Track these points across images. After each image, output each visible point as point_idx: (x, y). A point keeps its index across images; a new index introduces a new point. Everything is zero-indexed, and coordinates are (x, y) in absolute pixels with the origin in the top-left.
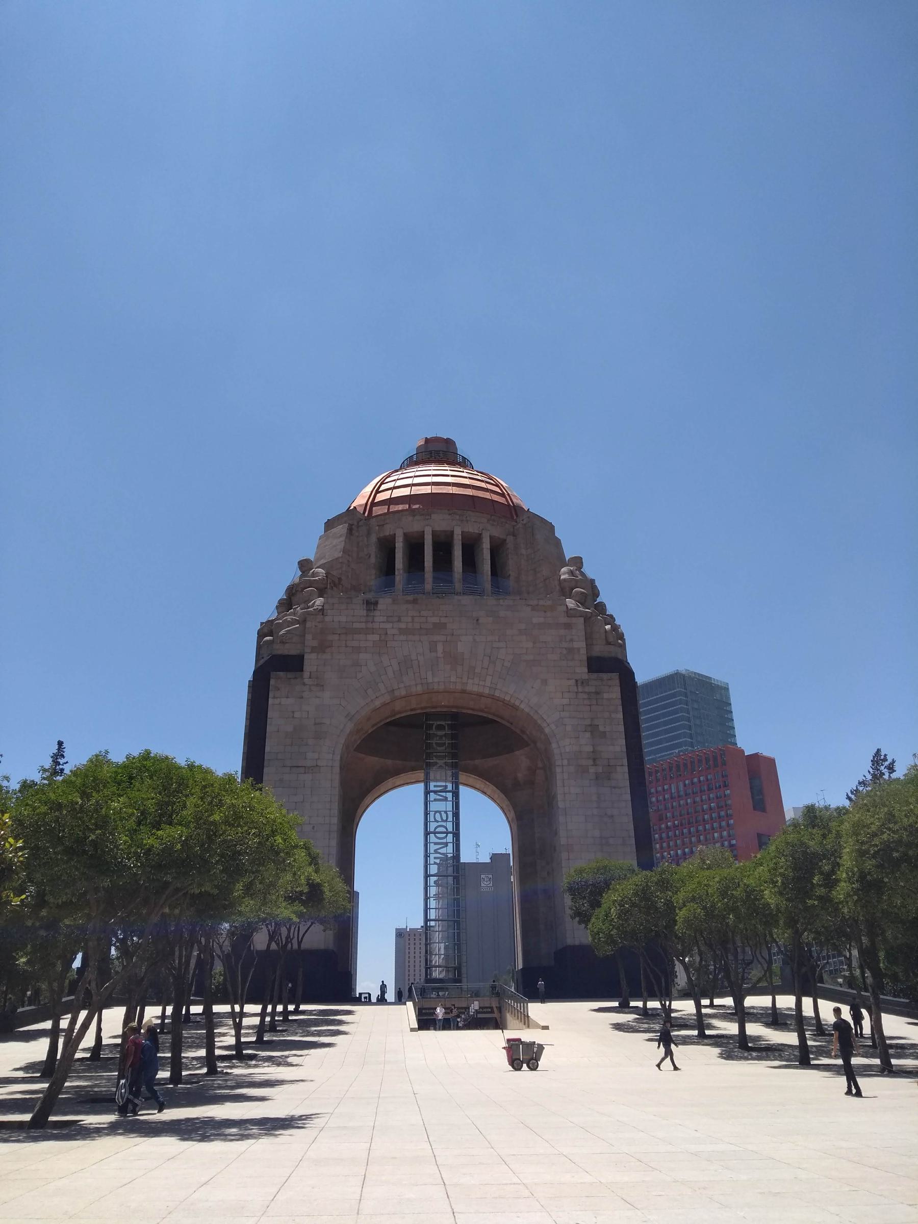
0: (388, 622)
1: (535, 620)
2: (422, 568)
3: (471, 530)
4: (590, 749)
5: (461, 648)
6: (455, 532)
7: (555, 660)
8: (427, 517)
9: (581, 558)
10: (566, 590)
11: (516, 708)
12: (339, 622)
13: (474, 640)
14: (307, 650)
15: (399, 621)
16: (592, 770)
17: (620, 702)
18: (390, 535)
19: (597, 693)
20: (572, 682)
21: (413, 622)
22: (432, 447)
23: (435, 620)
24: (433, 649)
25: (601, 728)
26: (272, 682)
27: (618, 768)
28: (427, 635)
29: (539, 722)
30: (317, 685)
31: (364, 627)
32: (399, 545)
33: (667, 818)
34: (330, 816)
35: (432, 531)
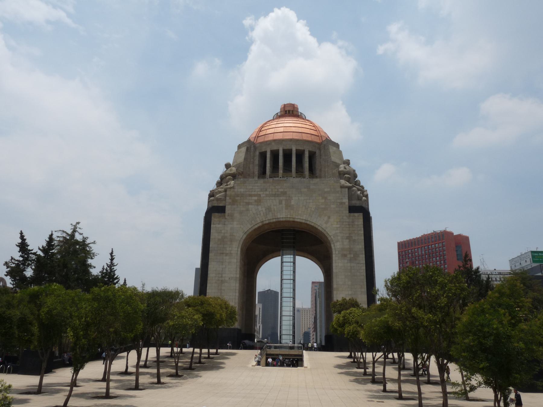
0: (261, 191)
1: (326, 190)
3: (300, 148)
4: (348, 247)
5: (293, 202)
6: (293, 150)
9: (349, 160)
10: (342, 175)
11: (316, 229)
12: (241, 192)
14: (227, 204)
15: (266, 190)
17: (362, 226)
18: (265, 151)
22: (287, 109)
25: (354, 238)
26: (212, 218)
28: (278, 197)
29: (326, 235)
32: (268, 155)
33: (416, 264)
34: (236, 274)
35: (283, 149)
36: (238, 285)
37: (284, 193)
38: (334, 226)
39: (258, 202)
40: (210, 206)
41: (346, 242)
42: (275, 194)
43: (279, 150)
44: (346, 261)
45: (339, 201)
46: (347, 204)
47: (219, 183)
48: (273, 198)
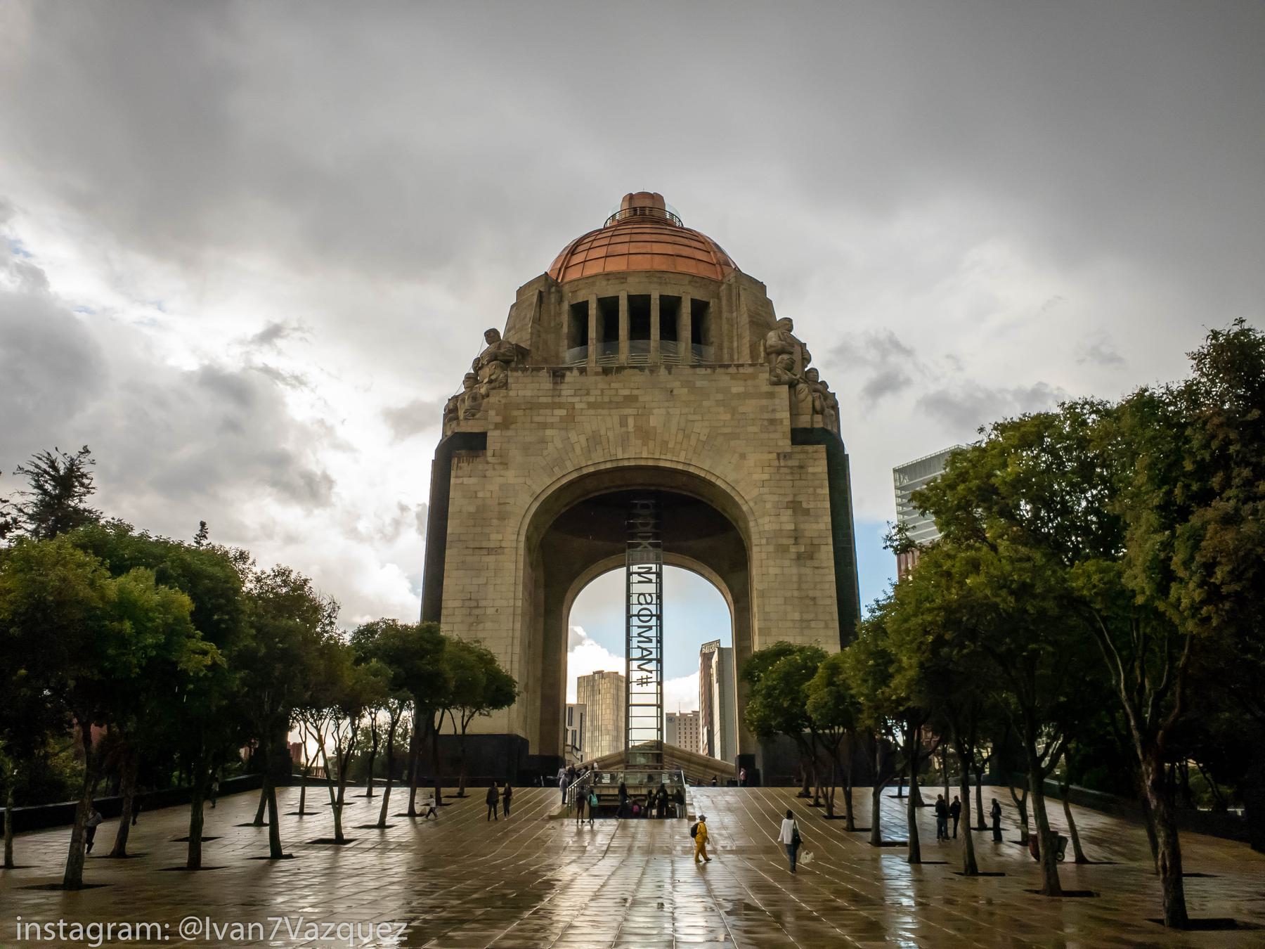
0: (575, 395)
1: (734, 390)
2: (616, 337)
4: (792, 527)
7: (755, 433)
8: (622, 281)
12: (524, 396)
13: (668, 413)
15: (588, 394)
16: (793, 549)
17: (826, 476)
18: (584, 302)
19: (801, 467)
20: (775, 455)
21: (602, 394)
23: (626, 392)
24: (623, 423)
25: (805, 505)
27: (822, 547)
30: (501, 463)
31: (550, 401)
36: (518, 625)
37: (631, 400)
38: (757, 477)
39: (570, 419)
40: (449, 433)
41: (786, 516)
42: (611, 402)
43: (617, 298)
44: (787, 563)
45: (766, 416)
46: (787, 422)
47: (470, 378)
48: (605, 412)
